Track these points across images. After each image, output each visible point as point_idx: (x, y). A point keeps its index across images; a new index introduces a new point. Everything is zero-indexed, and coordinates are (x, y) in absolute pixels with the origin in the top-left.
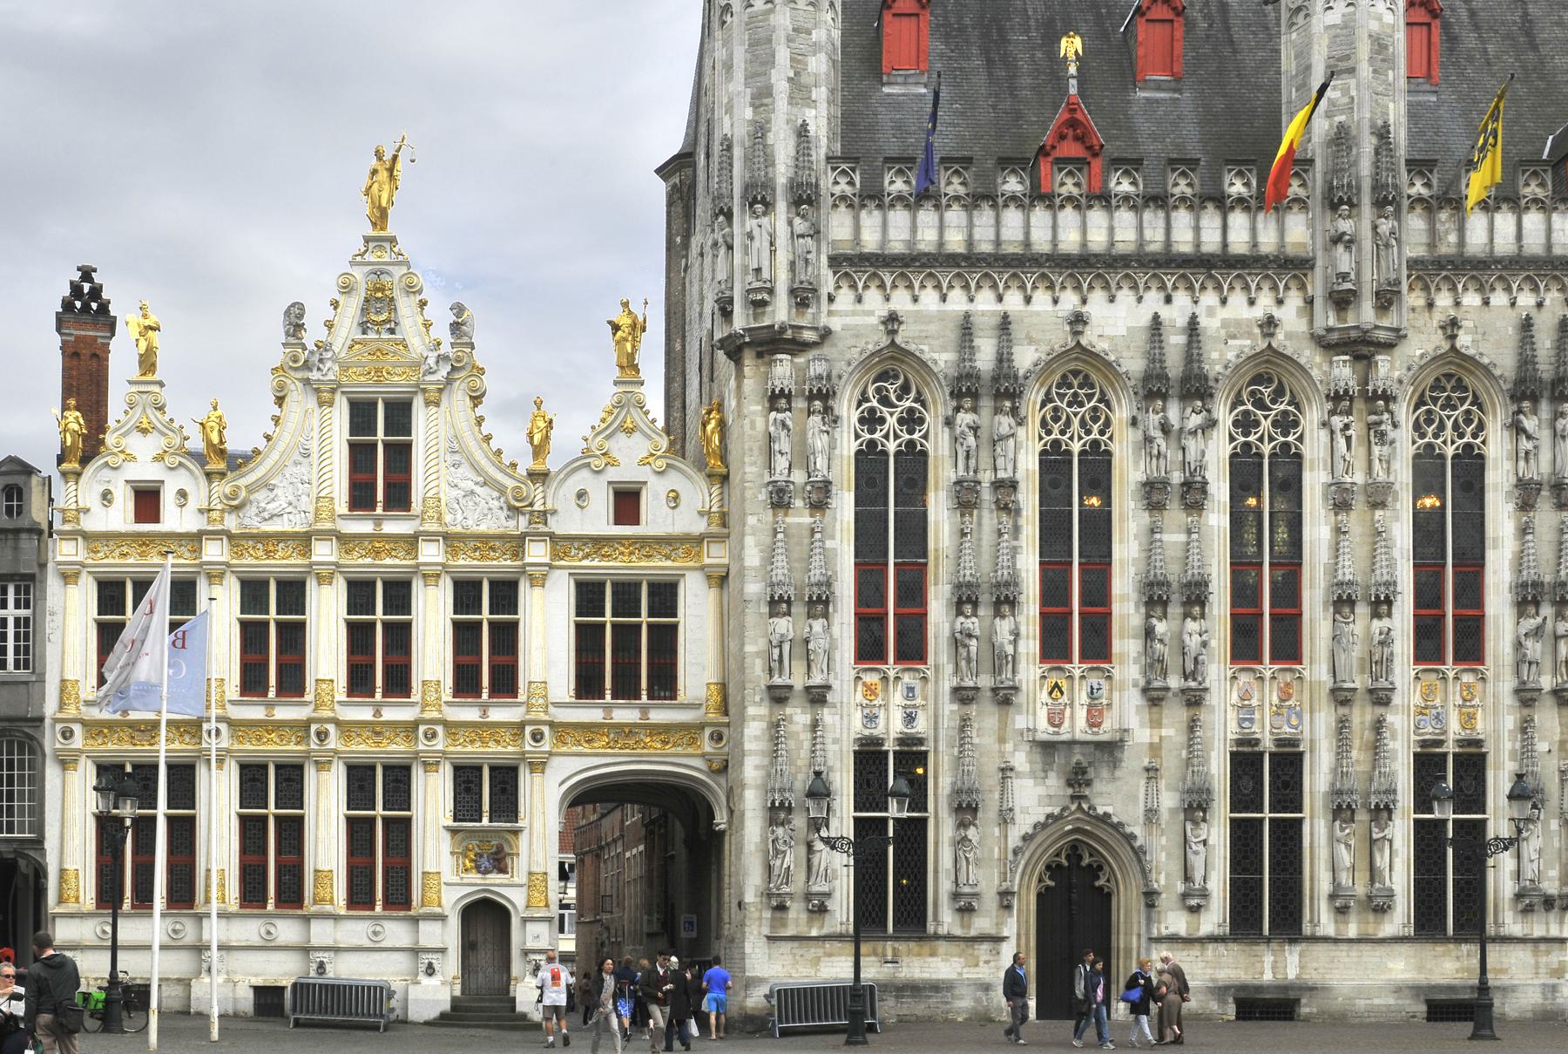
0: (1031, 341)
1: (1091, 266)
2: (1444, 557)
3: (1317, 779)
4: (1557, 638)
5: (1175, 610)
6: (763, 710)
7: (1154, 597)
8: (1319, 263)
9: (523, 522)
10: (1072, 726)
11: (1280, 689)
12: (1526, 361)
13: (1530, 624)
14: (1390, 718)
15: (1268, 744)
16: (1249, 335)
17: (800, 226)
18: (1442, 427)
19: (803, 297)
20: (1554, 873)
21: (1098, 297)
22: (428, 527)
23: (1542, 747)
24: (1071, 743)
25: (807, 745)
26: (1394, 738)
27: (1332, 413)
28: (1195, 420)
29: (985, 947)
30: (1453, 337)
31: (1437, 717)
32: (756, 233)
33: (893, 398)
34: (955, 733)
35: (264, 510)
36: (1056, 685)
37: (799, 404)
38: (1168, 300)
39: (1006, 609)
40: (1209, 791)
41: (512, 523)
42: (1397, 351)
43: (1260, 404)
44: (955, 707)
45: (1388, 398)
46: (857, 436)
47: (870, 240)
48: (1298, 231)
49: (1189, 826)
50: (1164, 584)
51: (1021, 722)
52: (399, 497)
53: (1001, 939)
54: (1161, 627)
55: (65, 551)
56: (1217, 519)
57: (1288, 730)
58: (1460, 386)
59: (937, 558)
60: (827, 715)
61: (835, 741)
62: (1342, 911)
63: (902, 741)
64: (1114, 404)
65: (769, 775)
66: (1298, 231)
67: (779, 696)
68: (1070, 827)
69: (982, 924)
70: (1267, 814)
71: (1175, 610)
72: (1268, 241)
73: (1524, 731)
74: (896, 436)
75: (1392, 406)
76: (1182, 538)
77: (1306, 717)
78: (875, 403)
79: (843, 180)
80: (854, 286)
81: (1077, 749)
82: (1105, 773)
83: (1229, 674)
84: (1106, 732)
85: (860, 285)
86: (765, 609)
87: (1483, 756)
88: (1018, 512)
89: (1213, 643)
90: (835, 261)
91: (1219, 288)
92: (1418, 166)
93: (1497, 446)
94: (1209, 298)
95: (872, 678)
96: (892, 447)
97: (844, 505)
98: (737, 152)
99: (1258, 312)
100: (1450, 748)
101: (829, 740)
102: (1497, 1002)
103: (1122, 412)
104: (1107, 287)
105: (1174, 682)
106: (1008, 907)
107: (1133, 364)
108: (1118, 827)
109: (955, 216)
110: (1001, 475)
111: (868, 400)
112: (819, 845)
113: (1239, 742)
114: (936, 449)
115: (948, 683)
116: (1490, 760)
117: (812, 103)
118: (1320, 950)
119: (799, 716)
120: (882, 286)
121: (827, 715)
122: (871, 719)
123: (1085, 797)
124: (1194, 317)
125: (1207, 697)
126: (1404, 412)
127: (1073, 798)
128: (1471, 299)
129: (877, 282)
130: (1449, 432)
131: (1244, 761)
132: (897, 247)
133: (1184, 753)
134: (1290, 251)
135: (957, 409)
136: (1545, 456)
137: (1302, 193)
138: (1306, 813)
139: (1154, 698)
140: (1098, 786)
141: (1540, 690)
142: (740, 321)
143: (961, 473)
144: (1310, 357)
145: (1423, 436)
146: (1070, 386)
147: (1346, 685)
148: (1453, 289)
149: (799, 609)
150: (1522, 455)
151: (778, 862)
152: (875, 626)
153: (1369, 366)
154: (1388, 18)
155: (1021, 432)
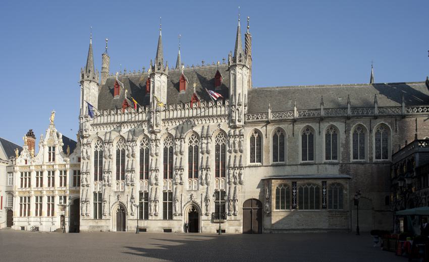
29: (108, 221)
42: (162, 133)
51: (112, 189)
53: (109, 220)
55: (17, 168)
69: (107, 218)
90: (91, 125)
96: (98, 150)
102: (172, 230)
109: (106, 118)
122: (95, 189)
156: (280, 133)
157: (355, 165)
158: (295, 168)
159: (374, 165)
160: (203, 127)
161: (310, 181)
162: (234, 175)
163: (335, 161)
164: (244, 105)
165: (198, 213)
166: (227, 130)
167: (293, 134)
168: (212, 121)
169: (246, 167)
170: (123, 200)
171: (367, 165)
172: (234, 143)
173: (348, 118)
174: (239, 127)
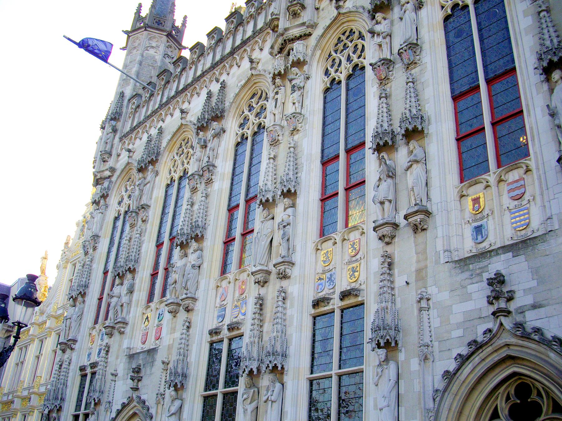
11: (240, 287)
14: (290, 290)
23: (399, 281)
26: (292, 306)
31: (330, 279)
36: (147, 318)
40: (185, 376)
57: (241, 317)
68: (131, 413)
75: (306, 68)
81: (141, 356)
82: (148, 372)
83: (213, 284)
89: (205, 266)
90: (121, 139)
95: (94, 333)
101: (70, 371)
125: (198, 303)
140: (143, 379)
141: (396, 226)
150: (377, 47)
155: (158, 178)
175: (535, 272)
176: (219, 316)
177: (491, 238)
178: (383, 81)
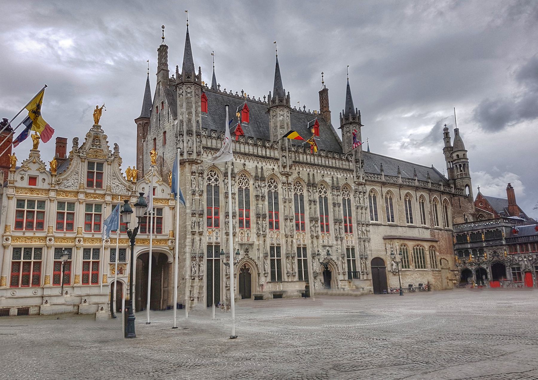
0: (237, 167)
1: (246, 155)
2: (299, 212)
3: (283, 252)
4: (316, 227)
5: (261, 219)
6: (190, 236)
7: (258, 216)
8: (280, 160)
9: (130, 193)
10: (245, 241)
12: (309, 180)
13: (312, 225)
15: (276, 245)
16: (270, 171)
17: (198, 140)
18: (297, 190)
19: (199, 154)
20: (318, 269)
21: (247, 160)
22: (108, 192)
23: (315, 246)
24: (245, 244)
25: (199, 244)
26: (294, 244)
27: (283, 186)
28: (263, 185)
30: (299, 175)
32: (190, 140)
33: (213, 175)
34: (226, 242)
35: (66, 185)
37: (197, 174)
38: (258, 163)
39: (234, 217)
41: (127, 193)
43: (272, 183)
44: (226, 236)
45: (291, 184)
46: (207, 182)
47: (209, 145)
48: (276, 154)
49: (265, 260)
50: (260, 214)
52: (99, 185)
54: (259, 222)
56: (266, 203)
58: (300, 183)
59: (222, 207)
60: (202, 238)
61: (204, 243)
62: (288, 276)
63: (216, 243)
64: (250, 180)
65: (192, 250)
66: (276, 154)
67: (193, 233)
70: (276, 258)
71: (261, 219)
72: (272, 155)
73: (312, 243)
74: (214, 183)
76: (262, 206)
77: (281, 240)
78: (210, 176)
79: (204, 132)
80: (206, 153)
84: (251, 241)
85: (208, 153)
86: (191, 215)
87: (306, 247)
88: (235, 199)
91: (265, 162)
92: (294, 146)
93: (305, 193)
94: (264, 164)
95: (209, 230)
96: (213, 185)
97: (205, 194)
98: (185, 124)
99: (271, 167)
100: (302, 246)
103: (251, 182)
104: (248, 159)
105: (261, 233)
106: (235, 277)
107: (254, 174)
108: (253, 260)
110: (233, 192)
111: (209, 175)
112: (201, 265)
113: (271, 244)
114: (221, 186)
115: (224, 232)
116: (307, 248)
117: (199, 117)
118: (286, 283)
119: (197, 238)
120: (211, 154)
121: (202, 238)
122: (210, 238)
123: (247, 255)
124: (262, 167)
126: (292, 186)
127: (246, 254)
128: (301, 169)
129: (210, 153)
130: (298, 191)
131: (272, 248)
132: (214, 147)
133: (263, 246)
134: (276, 157)
135: (225, 179)
136: (312, 196)
137: (277, 147)
138: (282, 257)
139: (258, 235)
140: (249, 252)
142: (185, 156)
143: (226, 191)
144: (279, 175)
145: (295, 191)
146: (243, 177)
147: (288, 234)
148: (298, 167)
149: (197, 215)
151: (194, 269)
152: (210, 220)
153: (288, 178)
154: (288, 120)
155: (236, 184)
156: (389, 195)
157: (437, 231)
158: (404, 229)
159: (446, 232)
160: (333, 178)
161: (419, 243)
162: (362, 232)
163: (426, 226)
164: (360, 162)
165: (331, 272)
166: (353, 186)
167: (400, 198)
168: (339, 173)
169: (370, 225)
170: (254, 254)
171: (443, 231)
172: (360, 199)
173: (430, 190)
174: (361, 184)
175: (332, 251)
176: (271, 240)
177: (325, 243)
178: (310, 204)
